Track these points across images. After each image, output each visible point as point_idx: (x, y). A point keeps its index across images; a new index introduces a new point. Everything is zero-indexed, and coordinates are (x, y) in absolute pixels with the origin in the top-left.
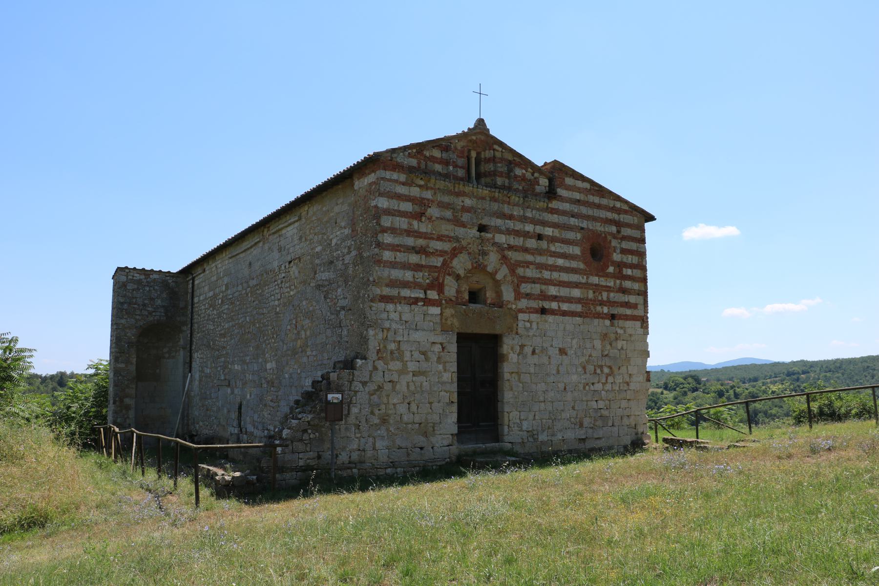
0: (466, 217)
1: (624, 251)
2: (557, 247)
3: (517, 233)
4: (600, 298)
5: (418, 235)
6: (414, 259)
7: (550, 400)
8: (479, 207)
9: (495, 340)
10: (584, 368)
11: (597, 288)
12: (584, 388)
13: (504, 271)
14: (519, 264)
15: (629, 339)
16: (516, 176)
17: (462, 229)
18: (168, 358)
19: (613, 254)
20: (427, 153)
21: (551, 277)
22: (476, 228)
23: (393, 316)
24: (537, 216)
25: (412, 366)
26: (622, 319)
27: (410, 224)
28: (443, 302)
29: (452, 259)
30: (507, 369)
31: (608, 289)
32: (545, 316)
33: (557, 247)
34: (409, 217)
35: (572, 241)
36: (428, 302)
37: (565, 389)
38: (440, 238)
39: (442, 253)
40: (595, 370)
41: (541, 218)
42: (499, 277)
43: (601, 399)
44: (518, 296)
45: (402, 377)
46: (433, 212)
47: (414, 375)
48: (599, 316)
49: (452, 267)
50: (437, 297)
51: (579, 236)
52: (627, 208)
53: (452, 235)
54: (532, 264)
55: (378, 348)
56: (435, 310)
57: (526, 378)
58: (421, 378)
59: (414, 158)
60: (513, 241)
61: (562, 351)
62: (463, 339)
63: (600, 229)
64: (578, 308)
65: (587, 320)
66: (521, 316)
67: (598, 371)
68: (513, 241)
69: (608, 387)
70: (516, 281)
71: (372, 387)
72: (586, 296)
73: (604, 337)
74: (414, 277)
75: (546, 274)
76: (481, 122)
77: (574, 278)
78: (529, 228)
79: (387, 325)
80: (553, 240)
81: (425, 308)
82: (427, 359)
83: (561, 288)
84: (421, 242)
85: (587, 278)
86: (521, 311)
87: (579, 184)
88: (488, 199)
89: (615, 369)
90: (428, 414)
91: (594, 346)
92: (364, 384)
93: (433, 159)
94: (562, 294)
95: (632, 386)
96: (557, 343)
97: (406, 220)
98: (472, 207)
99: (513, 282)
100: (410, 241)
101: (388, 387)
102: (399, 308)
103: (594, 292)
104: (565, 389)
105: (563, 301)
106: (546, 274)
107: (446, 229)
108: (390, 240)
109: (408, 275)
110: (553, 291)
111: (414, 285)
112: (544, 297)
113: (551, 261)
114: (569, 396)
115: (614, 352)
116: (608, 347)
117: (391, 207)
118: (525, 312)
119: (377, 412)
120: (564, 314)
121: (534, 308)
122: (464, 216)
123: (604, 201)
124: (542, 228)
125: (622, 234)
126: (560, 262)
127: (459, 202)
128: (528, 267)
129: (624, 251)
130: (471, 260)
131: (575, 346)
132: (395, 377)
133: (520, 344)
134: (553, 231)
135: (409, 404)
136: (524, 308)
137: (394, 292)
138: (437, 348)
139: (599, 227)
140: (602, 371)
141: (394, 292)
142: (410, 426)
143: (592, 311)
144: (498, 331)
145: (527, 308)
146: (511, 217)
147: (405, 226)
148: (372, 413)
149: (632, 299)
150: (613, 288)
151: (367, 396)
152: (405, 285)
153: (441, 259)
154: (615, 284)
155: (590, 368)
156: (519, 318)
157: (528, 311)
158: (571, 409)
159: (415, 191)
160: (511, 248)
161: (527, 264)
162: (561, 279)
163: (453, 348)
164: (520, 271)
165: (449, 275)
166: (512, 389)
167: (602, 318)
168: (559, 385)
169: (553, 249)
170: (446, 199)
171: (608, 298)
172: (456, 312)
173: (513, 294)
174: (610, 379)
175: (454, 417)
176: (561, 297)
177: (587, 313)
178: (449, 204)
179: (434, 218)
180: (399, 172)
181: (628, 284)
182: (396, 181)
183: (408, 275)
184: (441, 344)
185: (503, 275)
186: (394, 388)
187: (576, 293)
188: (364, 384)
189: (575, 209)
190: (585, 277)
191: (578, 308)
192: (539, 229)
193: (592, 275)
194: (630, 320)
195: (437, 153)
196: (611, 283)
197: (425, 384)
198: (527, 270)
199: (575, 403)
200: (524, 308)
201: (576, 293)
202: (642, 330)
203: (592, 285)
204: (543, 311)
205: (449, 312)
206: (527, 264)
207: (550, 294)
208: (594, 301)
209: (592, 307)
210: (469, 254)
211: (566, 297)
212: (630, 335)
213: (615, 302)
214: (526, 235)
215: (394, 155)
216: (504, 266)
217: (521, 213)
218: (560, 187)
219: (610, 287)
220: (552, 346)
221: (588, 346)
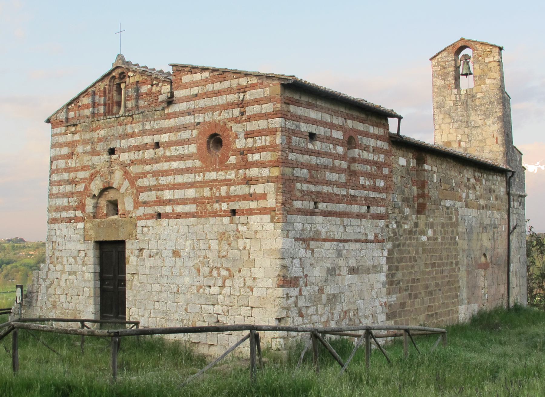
1: (248, 135)
2: (173, 151)
3: (137, 148)
4: (218, 194)
6: (69, 188)
7: (163, 300)
8: (109, 134)
10: (199, 270)
11: (213, 184)
12: (198, 291)
13: (126, 184)
15: (253, 237)
17: (97, 157)
19: (235, 142)
20: (80, 104)
21: (166, 182)
22: (107, 153)
23: (58, 232)
25: (68, 268)
26: (244, 215)
27: (67, 163)
28: (86, 218)
29: (90, 183)
30: (129, 269)
31: (228, 183)
32: (159, 220)
33: (173, 151)
35: (187, 140)
36: (77, 219)
37: (178, 291)
38: (83, 169)
39: (84, 180)
40: (211, 272)
42: (122, 190)
43: (218, 304)
44: (137, 204)
45: (63, 275)
47: (69, 275)
48: (216, 214)
49: (90, 190)
50: (81, 215)
51: (195, 132)
52: (256, 81)
53: (90, 164)
54: (149, 173)
55: (50, 255)
56: (80, 225)
57: (143, 278)
59: (72, 111)
61: (176, 253)
63: (219, 118)
64: (192, 208)
65: (203, 220)
66: (140, 223)
69: (226, 291)
70: (135, 192)
71: (48, 282)
72: (202, 194)
73: (222, 236)
74: (68, 202)
75: (163, 180)
76: (120, 57)
77: (189, 178)
78: (148, 139)
79: (54, 240)
80: (168, 145)
81: (75, 224)
83: (176, 191)
84: (72, 175)
85: (204, 176)
86: (139, 218)
87: (198, 77)
88: (116, 124)
89: (234, 270)
90: (76, 304)
91: (209, 247)
92: (44, 280)
94: (177, 197)
96: (171, 246)
97: (64, 161)
98: (104, 137)
99: (133, 193)
100: (66, 176)
101: (56, 282)
103: (211, 189)
104: (178, 291)
105: (178, 204)
106: (163, 180)
107: (87, 160)
108: (56, 178)
112: (160, 202)
113: (165, 166)
114: (181, 298)
115: (233, 253)
116: (227, 247)
117: (57, 154)
118: (142, 219)
119: (50, 300)
120: (178, 216)
121: (150, 214)
123: (226, 84)
124: (159, 136)
125: (247, 114)
126: (175, 165)
128: (146, 177)
129: (248, 135)
130: (102, 181)
131: (189, 248)
133: (138, 248)
134: (169, 136)
135: (67, 295)
136: (142, 215)
138: (82, 254)
139: (217, 117)
140: (219, 274)
142: (67, 311)
143: (207, 210)
144: (121, 238)
145: (144, 215)
146: (132, 135)
147: (63, 166)
148: (48, 300)
149: (258, 189)
150: (234, 180)
151: (45, 289)
152: (64, 209)
153: (83, 185)
154: (237, 174)
155: (206, 270)
156: (138, 225)
157: (145, 217)
158: (184, 311)
159: (70, 138)
161: (144, 175)
162: (176, 182)
164: (141, 182)
165: (88, 196)
166: (131, 289)
167: (220, 216)
168: (172, 286)
169: (168, 153)
170: (87, 136)
171: (227, 193)
172: (93, 225)
173: (133, 204)
174: (228, 283)
176: (177, 200)
177: (201, 213)
178: (89, 140)
179: (80, 154)
180: (61, 126)
181: (254, 172)
183: (64, 202)
184: (84, 250)
186: (59, 282)
187: (191, 193)
188: (44, 280)
189: (192, 105)
190: (202, 174)
191: (192, 208)
192: (157, 138)
193: (208, 171)
194: (255, 214)
195: (86, 101)
196: (231, 175)
197: (75, 281)
198: (145, 179)
199: (187, 305)
200: (142, 215)
201: (191, 193)
202: (272, 224)
203: (209, 181)
204: (159, 216)
205: (89, 225)
206: (144, 175)
207: (165, 198)
208: (211, 198)
209: (208, 206)
210: (101, 176)
212: (256, 232)
213: (235, 196)
214: (145, 147)
215: (58, 115)
218: (177, 88)
219: (231, 180)
220: (166, 249)
221: (202, 247)
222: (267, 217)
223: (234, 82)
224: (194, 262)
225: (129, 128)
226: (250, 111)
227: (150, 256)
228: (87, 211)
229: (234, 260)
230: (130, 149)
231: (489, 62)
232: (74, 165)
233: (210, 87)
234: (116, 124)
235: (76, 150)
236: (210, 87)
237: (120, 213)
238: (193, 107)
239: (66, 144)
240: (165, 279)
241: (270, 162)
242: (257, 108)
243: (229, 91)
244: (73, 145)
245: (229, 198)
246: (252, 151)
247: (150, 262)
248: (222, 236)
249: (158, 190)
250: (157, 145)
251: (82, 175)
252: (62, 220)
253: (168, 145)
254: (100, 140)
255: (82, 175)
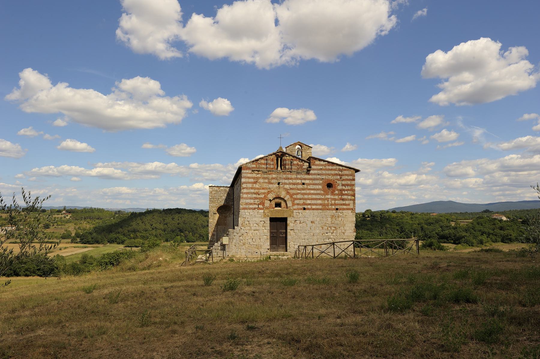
0: (273, 181)
1: (343, 185)
2: (311, 187)
3: (294, 184)
5: (255, 189)
9: (285, 220)
10: (323, 228)
12: (322, 235)
13: (288, 196)
14: (294, 194)
16: (294, 164)
17: (272, 185)
18: (229, 217)
24: (302, 177)
25: (253, 228)
30: (289, 228)
31: (335, 200)
33: (311, 187)
34: (252, 184)
36: (259, 209)
38: (263, 189)
39: (264, 193)
41: (304, 177)
46: (261, 180)
51: (321, 182)
58: (257, 232)
60: (291, 186)
62: (272, 220)
64: (320, 207)
65: (325, 211)
67: (329, 228)
68: (291, 186)
69: (334, 234)
71: (240, 234)
72: (324, 202)
73: (332, 217)
75: (306, 197)
78: (299, 181)
79: (245, 216)
80: (309, 184)
82: (259, 226)
84: (256, 191)
86: (295, 209)
87: (322, 163)
89: (338, 227)
92: (238, 233)
93: (261, 164)
95: (346, 234)
98: (276, 177)
100: (252, 191)
102: (249, 211)
106: (306, 197)
107: (265, 186)
109: (252, 201)
110: (309, 202)
111: (255, 204)
112: (304, 204)
113: (308, 192)
114: (315, 237)
118: (297, 210)
120: (314, 209)
122: (272, 180)
123: (334, 167)
126: (312, 192)
127: (270, 176)
129: (343, 185)
132: (248, 231)
137: (247, 206)
139: (330, 177)
141: (247, 206)
145: (297, 208)
149: (347, 202)
152: (251, 204)
153: (264, 195)
156: (294, 212)
160: (291, 189)
161: (298, 194)
163: (269, 222)
164: (295, 196)
165: (267, 200)
166: (290, 235)
168: (311, 233)
169: (309, 187)
170: (265, 176)
174: (335, 232)
175: (269, 243)
179: (261, 183)
182: (248, 173)
183: (252, 201)
184: (264, 221)
185: (287, 198)
188: (238, 233)
189: (320, 172)
190: (324, 196)
191: (320, 207)
192: (303, 181)
195: (263, 161)
196: (336, 197)
204: (304, 209)
206: (298, 194)
208: (328, 204)
211: (314, 204)
212: (346, 215)
214: (298, 184)
216: (288, 195)
217: (296, 177)
219: (336, 199)
222: (350, 211)
223: (338, 167)
224: (321, 225)
225: (289, 176)
226: (344, 177)
227: (300, 223)
228: (266, 206)
229: (337, 224)
230: (290, 184)
231: (308, 152)
232: (258, 187)
233: (328, 167)
234: (282, 173)
235: (259, 181)
236: (328, 167)
237: (282, 207)
238: (320, 173)
239: (254, 178)
240: (308, 231)
241: (351, 194)
242: (347, 177)
243: (335, 170)
244: (258, 178)
245: (335, 204)
246: (344, 190)
247: (299, 226)
248: (332, 217)
249: (304, 200)
250: (303, 184)
251: (263, 191)
252: (250, 209)
253: (309, 184)
254: (273, 178)
255: (263, 191)
